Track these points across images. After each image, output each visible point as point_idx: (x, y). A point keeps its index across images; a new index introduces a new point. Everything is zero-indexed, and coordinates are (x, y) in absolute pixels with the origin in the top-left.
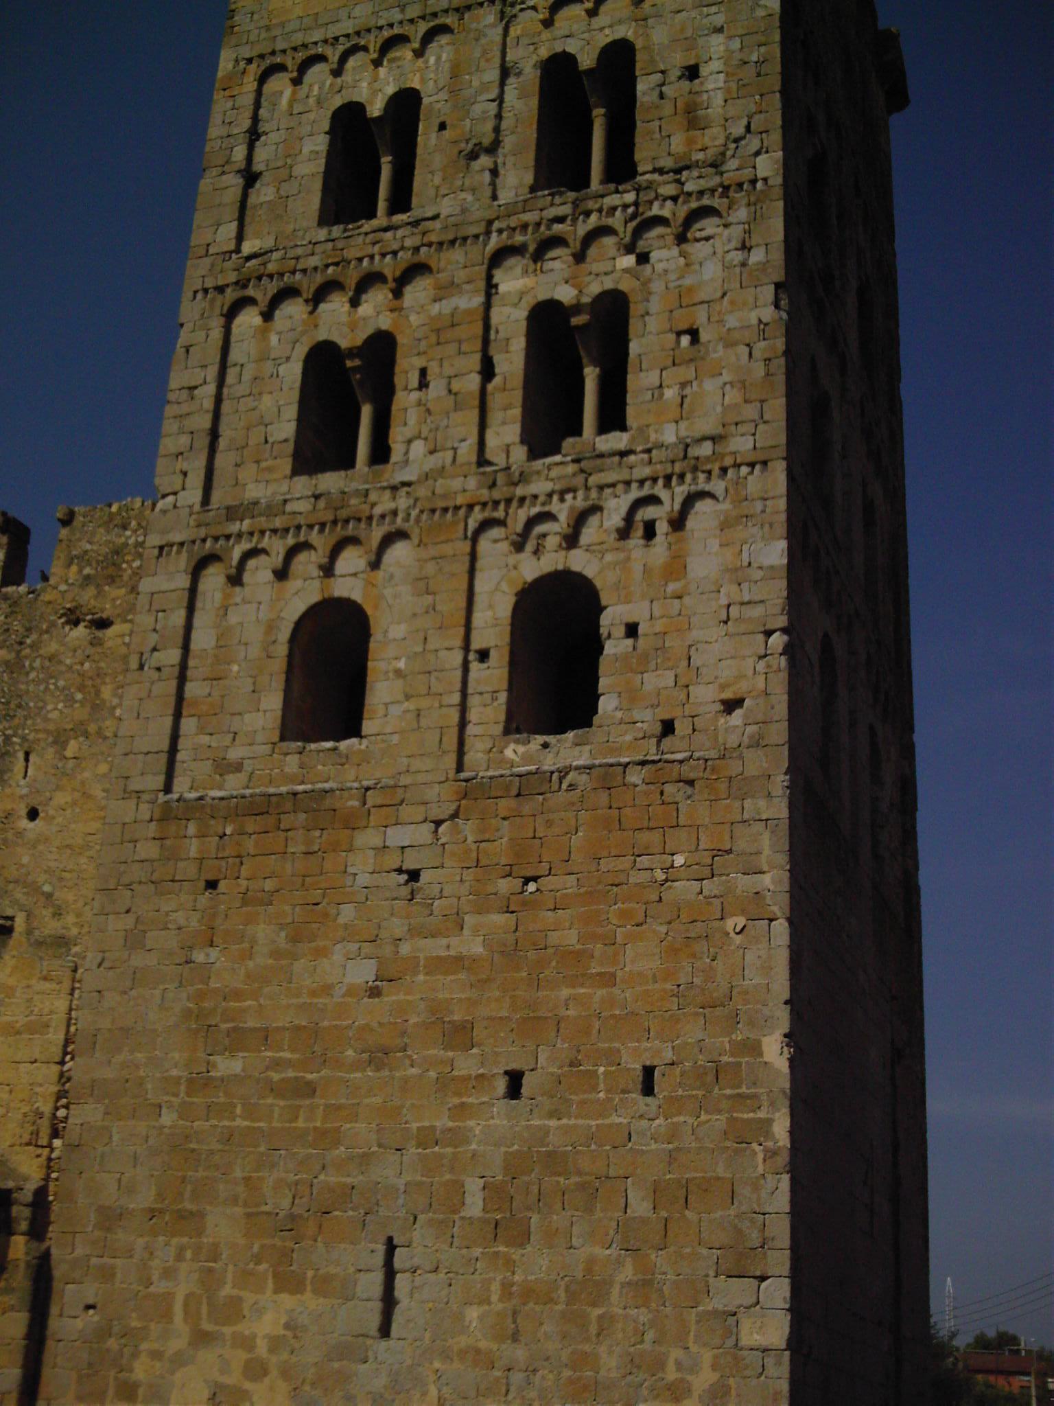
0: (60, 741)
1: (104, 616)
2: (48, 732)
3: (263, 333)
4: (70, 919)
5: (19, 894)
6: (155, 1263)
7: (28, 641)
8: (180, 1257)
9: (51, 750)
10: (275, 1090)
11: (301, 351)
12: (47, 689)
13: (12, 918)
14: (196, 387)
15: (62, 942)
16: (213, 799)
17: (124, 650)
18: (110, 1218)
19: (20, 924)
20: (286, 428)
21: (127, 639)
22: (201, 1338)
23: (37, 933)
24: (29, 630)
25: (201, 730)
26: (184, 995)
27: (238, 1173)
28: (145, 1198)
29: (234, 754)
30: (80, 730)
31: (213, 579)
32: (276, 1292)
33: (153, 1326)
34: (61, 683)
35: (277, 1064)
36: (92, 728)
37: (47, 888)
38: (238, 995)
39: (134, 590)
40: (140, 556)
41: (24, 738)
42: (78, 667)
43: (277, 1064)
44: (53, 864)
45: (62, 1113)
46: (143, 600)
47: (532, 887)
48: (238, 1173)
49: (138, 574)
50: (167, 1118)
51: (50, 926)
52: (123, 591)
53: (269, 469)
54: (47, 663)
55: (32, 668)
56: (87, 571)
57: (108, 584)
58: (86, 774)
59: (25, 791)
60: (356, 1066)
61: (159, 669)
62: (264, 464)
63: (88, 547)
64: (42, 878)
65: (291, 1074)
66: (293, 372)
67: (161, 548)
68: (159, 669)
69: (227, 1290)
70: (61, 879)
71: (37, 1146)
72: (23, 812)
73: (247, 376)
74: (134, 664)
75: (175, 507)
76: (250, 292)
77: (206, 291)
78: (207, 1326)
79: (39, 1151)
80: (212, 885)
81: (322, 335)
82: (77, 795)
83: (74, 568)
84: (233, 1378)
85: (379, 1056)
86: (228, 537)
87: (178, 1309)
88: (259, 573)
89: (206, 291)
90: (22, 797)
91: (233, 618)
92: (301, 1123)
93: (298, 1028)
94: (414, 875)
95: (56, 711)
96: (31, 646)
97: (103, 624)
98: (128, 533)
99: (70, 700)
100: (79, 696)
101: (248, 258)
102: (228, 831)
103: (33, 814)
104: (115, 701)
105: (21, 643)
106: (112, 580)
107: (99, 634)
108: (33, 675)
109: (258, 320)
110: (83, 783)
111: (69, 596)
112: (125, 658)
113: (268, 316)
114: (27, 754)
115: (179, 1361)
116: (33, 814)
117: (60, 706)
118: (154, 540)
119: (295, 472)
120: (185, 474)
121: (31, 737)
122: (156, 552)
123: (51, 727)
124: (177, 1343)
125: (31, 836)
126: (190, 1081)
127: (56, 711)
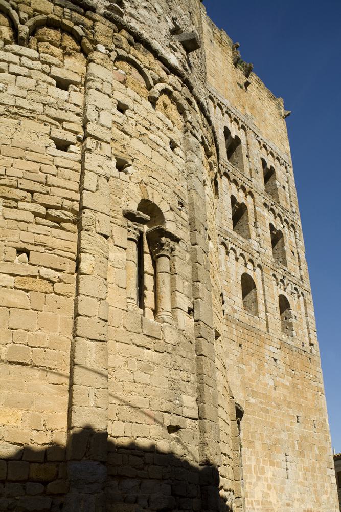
8: (251, 455)
10: (262, 409)
22: (258, 478)
27: (258, 432)
32: (270, 466)
33: (248, 474)
35: (261, 403)
38: (250, 380)
43: (261, 403)
47: (293, 372)
48: (258, 432)
60: (275, 408)
65: (264, 406)
69: (261, 465)
78: (259, 475)
84: (266, 490)
85: (278, 406)
87: (253, 470)
92: (267, 420)
93: (263, 394)
94: (275, 360)
115: (256, 485)
124: (254, 480)
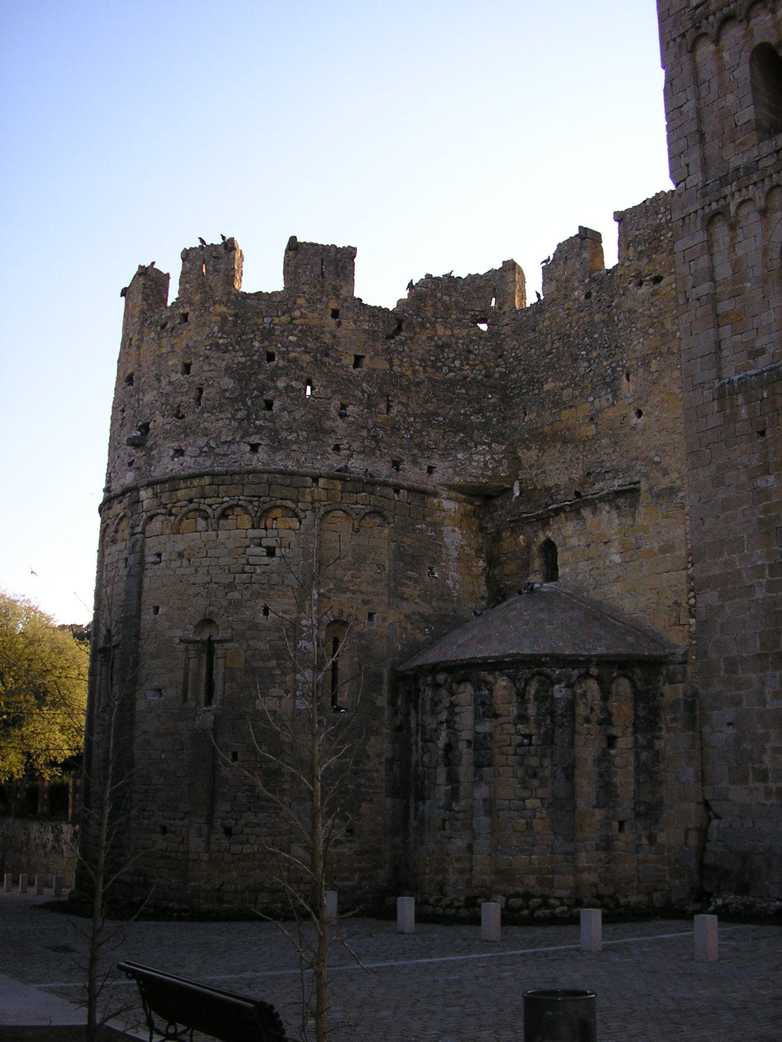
0: (646, 363)
1: (657, 275)
2: (637, 358)
3: (718, 52)
4: (675, 476)
5: (639, 466)
6: (767, 690)
7: (614, 304)
9: (641, 370)
11: (746, 55)
12: (631, 331)
13: (638, 482)
14: (682, 106)
15: (672, 491)
16: (751, 376)
17: (674, 293)
18: (732, 665)
19: (644, 486)
20: (748, 114)
21: (674, 286)
23: (655, 489)
24: (612, 296)
25: (734, 333)
26: (757, 510)
28: (756, 647)
29: (758, 344)
30: (657, 353)
31: (721, 231)
33: (772, 731)
34: (639, 325)
36: (664, 349)
37: (657, 459)
39: (671, 252)
40: (671, 229)
41: (623, 366)
42: (647, 312)
44: (658, 443)
45: (692, 601)
46: (679, 257)
49: (672, 241)
50: (760, 594)
51: (665, 483)
52: (665, 254)
53: (742, 144)
54: (628, 314)
55: (620, 321)
56: (640, 249)
57: (655, 253)
58: (666, 380)
59: (631, 400)
61: (698, 299)
62: (737, 142)
63: (638, 233)
64: (652, 453)
66: (743, 72)
67: (683, 218)
68: (698, 299)
70: (664, 451)
71: (680, 625)
72: (633, 414)
73: (714, 88)
74: (681, 301)
75: (686, 189)
76: (703, 30)
77: (674, 40)
79: (681, 628)
80: (762, 433)
81: (758, 41)
82: (663, 395)
83: (631, 249)
86: (725, 197)
88: (750, 218)
89: (674, 40)
90: (630, 404)
91: (740, 252)
95: (639, 345)
96: (616, 307)
97: (657, 280)
98: (660, 216)
99: (646, 334)
100: (651, 331)
101: (697, 7)
102: (765, 396)
103: (639, 414)
104: (675, 328)
105: (609, 307)
106: (656, 250)
107: (656, 287)
108: (620, 325)
109: (712, 47)
110: (665, 386)
111: (632, 268)
112: (675, 299)
113: (716, 41)
114: (628, 376)
116: (639, 414)
117: (641, 340)
118: (677, 215)
119: (761, 140)
120: (688, 165)
121: (627, 365)
122: (680, 222)
123: (638, 354)
125: (640, 427)
126: (771, 567)
127: (639, 345)
